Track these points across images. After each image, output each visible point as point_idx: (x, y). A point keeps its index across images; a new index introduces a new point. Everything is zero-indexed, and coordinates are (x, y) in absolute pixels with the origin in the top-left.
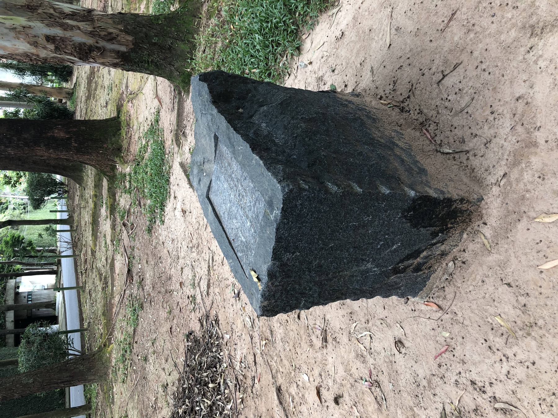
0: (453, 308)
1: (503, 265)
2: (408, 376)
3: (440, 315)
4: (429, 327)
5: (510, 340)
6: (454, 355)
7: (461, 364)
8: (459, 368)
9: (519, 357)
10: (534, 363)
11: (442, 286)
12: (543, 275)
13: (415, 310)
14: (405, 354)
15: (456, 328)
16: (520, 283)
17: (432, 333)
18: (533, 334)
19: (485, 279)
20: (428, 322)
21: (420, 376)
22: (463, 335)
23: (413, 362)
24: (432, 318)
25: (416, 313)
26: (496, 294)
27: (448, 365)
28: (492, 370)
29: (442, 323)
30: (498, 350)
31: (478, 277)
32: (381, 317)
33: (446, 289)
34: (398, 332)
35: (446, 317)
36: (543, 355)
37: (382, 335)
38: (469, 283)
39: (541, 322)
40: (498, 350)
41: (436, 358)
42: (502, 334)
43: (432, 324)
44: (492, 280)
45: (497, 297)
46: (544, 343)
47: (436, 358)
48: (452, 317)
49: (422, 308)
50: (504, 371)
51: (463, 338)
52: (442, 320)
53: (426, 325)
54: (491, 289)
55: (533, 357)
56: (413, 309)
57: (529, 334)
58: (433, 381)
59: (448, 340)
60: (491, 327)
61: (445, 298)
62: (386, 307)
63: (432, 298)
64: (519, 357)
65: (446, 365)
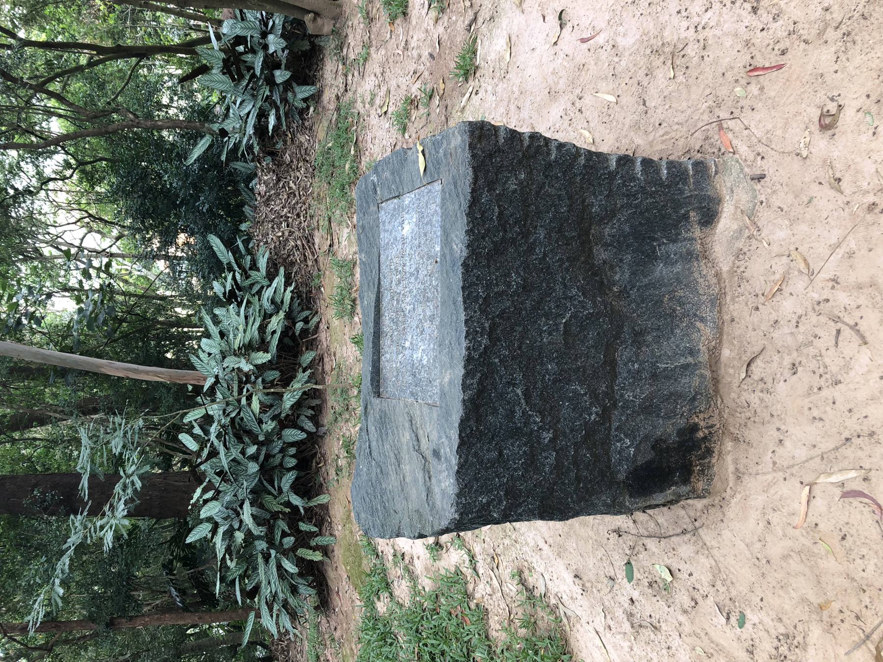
0: (706, 117)
1: (636, 127)
2: (858, 60)
3: (730, 122)
4: (757, 116)
5: (681, 46)
6: (752, 58)
7: (752, 41)
8: (759, 38)
9: (685, 24)
10: (679, 12)
11: (699, 155)
12: (620, 93)
13: (759, 154)
14: (832, 100)
15: (723, 92)
16: (635, 99)
17: (759, 106)
18: (661, 43)
19: (657, 125)
20: (752, 125)
21: (833, 49)
22: (721, 79)
23: (828, 78)
24: (742, 126)
25: (761, 149)
26: (659, 102)
27: (771, 47)
28: (722, 19)
29: (734, 110)
30: (698, 41)
31: (661, 132)
32: (832, 193)
33: (697, 148)
34: (821, 144)
35: (724, 115)
36: (667, 17)
37: (858, 160)
38: (673, 134)
39: (648, 51)
40: (698, 41)
41: (780, 67)
42: (683, 56)
43: (748, 118)
44: (652, 120)
45: (660, 100)
46: (659, 30)
47: (780, 67)
48: (717, 110)
49: (746, 148)
50: (710, 13)
51: (724, 74)
52: (732, 113)
53: (760, 122)
54: (659, 111)
55: (676, 20)
56: (759, 158)
57: (663, 44)
58: (814, 32)
59: (743, 82)
60: (688, 72)
61: (707, 138)
62: (806, 200)
63: (720, 150)
64: (685, 24)
65: (773, 49)
